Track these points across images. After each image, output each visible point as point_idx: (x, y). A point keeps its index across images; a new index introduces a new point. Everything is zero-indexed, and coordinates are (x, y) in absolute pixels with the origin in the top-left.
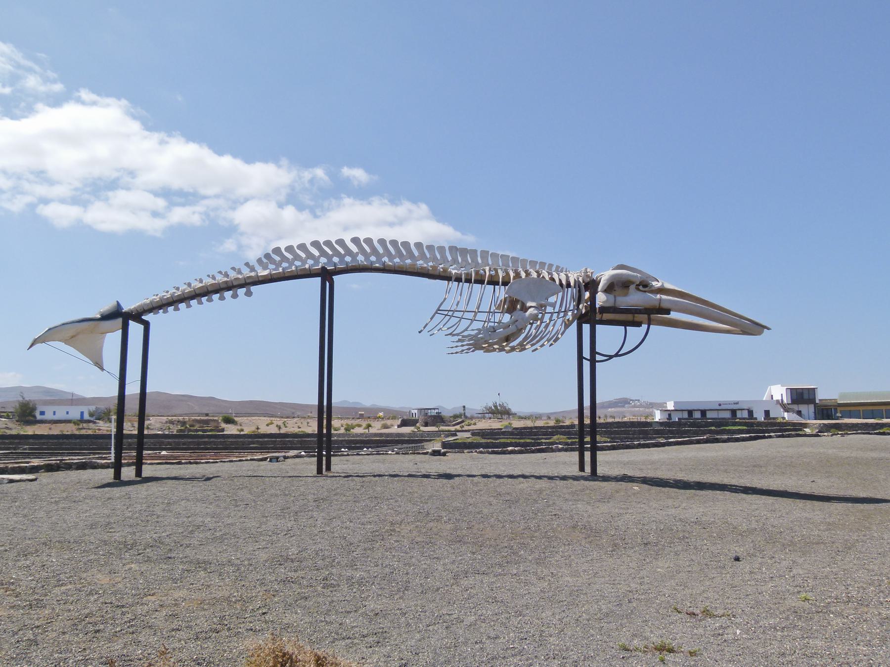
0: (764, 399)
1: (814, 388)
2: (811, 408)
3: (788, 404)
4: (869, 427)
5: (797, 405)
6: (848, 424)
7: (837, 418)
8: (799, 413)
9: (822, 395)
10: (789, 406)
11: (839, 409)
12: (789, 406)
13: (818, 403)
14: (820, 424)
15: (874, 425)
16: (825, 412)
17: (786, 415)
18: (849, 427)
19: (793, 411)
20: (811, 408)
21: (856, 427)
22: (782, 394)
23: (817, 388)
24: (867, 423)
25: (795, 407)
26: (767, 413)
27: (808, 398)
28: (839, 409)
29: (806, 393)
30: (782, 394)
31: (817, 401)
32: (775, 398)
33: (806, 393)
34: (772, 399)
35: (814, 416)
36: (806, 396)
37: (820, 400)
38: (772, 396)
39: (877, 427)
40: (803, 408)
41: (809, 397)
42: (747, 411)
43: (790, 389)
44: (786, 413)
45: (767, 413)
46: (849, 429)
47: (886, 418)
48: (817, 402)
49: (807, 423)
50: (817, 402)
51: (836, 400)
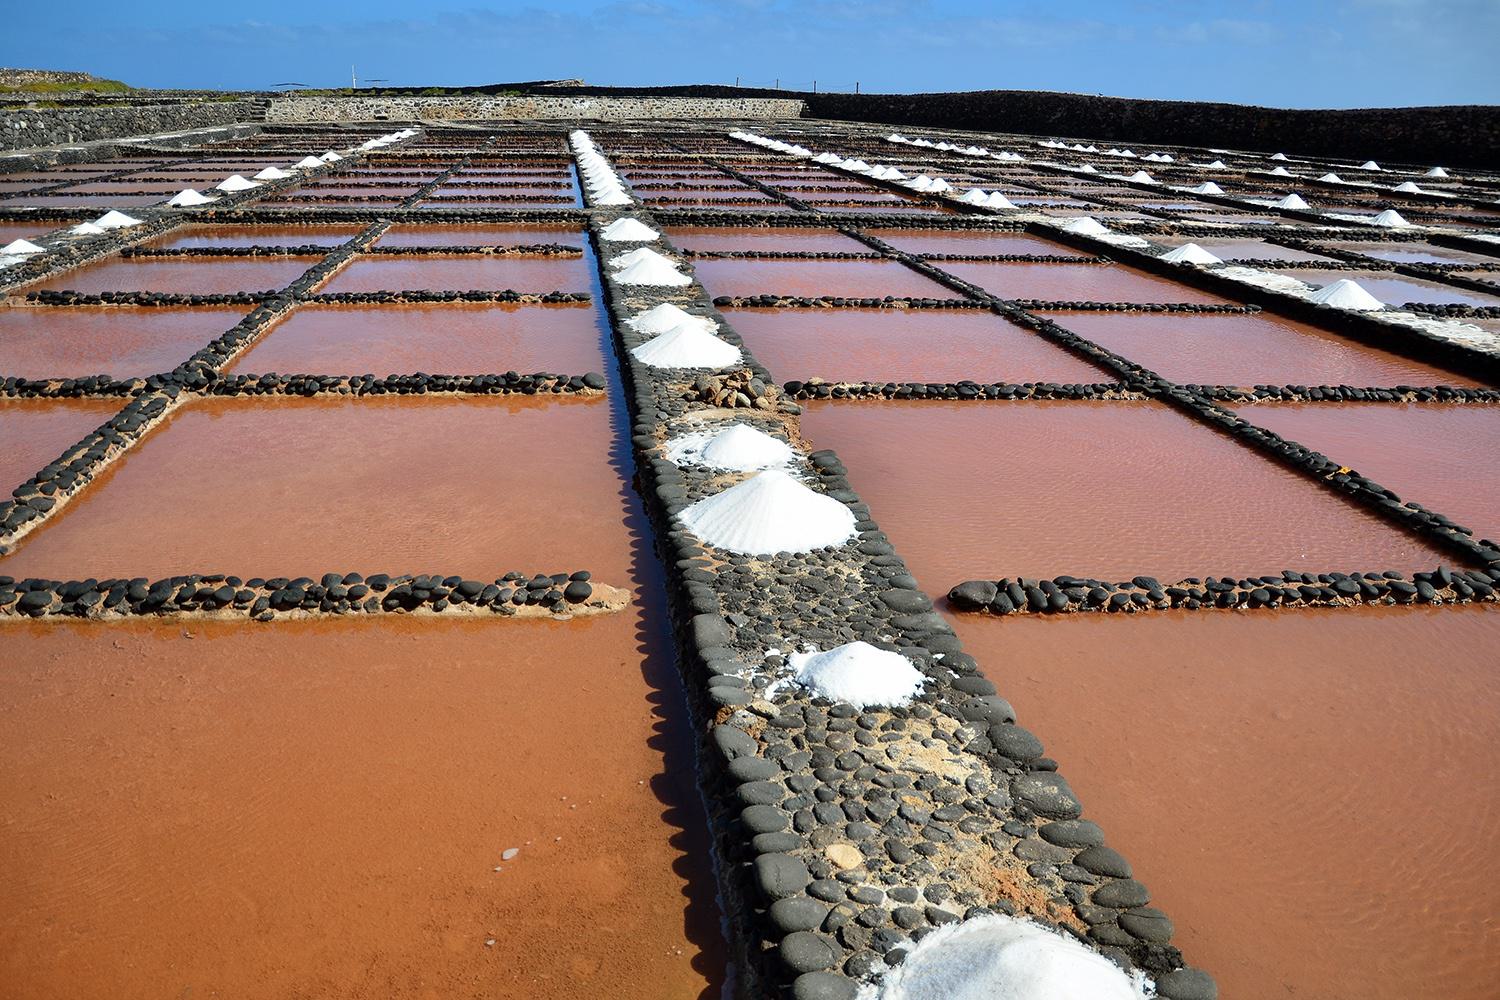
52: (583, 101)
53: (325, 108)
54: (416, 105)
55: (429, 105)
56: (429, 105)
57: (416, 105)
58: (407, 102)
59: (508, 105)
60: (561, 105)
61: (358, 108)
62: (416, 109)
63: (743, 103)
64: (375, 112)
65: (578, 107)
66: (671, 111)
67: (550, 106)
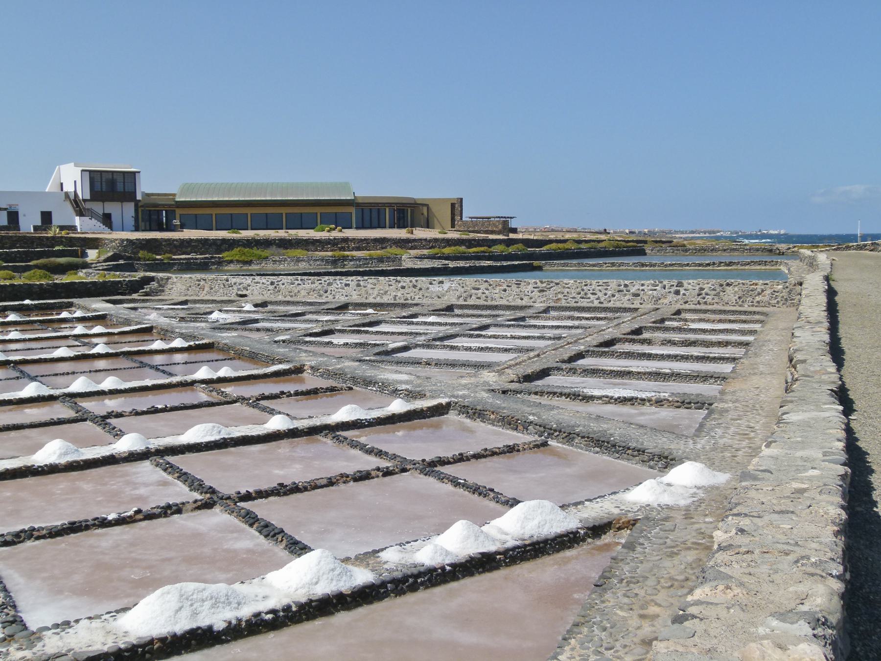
0: (47, 190)
1: (134, 174)
2: (129, 209)
3: (85, 201)
4: (210, 245)
5: (100, 204)
6: (174, 240)
7: (170, 228)
8: (107, 220)
9: (145, 187)
10: (88, 205)
11: (179, 212)
12: (88, 205)
13: (139, 201)
14: (123, 240)
15: (219, 243)
16: (154, 217)
17: (77, 221)
18: (175, 246)
19: (92, 214)
20: (129, 209)
21: (187, 247)
22: (75, 182)
23: (139, 172)
24: (206, 240)
25: (98, 207)
26: (47, 217)
27: (100, 190)
28: (179, 212)
29: (120, 179)
30: (75, 182)
31: (139, 197)
32: (65, 190)
33: (120, 179)
34: (62, 190)
35: (133, 223)
36: (120, 187)
37: (143, 193)
38: (62, 184)
39: (224, 246)
40: (113, 208)
41: (124, 189)
42: (5, 213)
43: (90, 171)
44: (77, 218)
45: (47, 217)
46: (174, 250)
47: (217, 229)
48: (138, 198)
49: (97, 239)
50: (138, 198)
51: (174, 195)
52: (441, 282)
53: (199, 285)
54: (272, 283)
55: (283, 284)
56: (283, 284)
57: (272, 283)
58: (264, 281)
59: (359, 285)
60: (415, 286)
61: (224, 285)
62: (271, 287)
63: (680, 284)
64: (239, 289)
65: (435, 288)
66: (560, 296)
67: (403, 287)
